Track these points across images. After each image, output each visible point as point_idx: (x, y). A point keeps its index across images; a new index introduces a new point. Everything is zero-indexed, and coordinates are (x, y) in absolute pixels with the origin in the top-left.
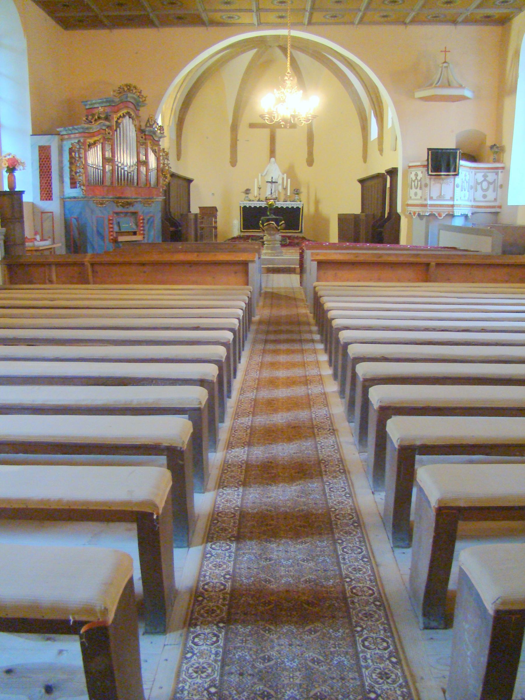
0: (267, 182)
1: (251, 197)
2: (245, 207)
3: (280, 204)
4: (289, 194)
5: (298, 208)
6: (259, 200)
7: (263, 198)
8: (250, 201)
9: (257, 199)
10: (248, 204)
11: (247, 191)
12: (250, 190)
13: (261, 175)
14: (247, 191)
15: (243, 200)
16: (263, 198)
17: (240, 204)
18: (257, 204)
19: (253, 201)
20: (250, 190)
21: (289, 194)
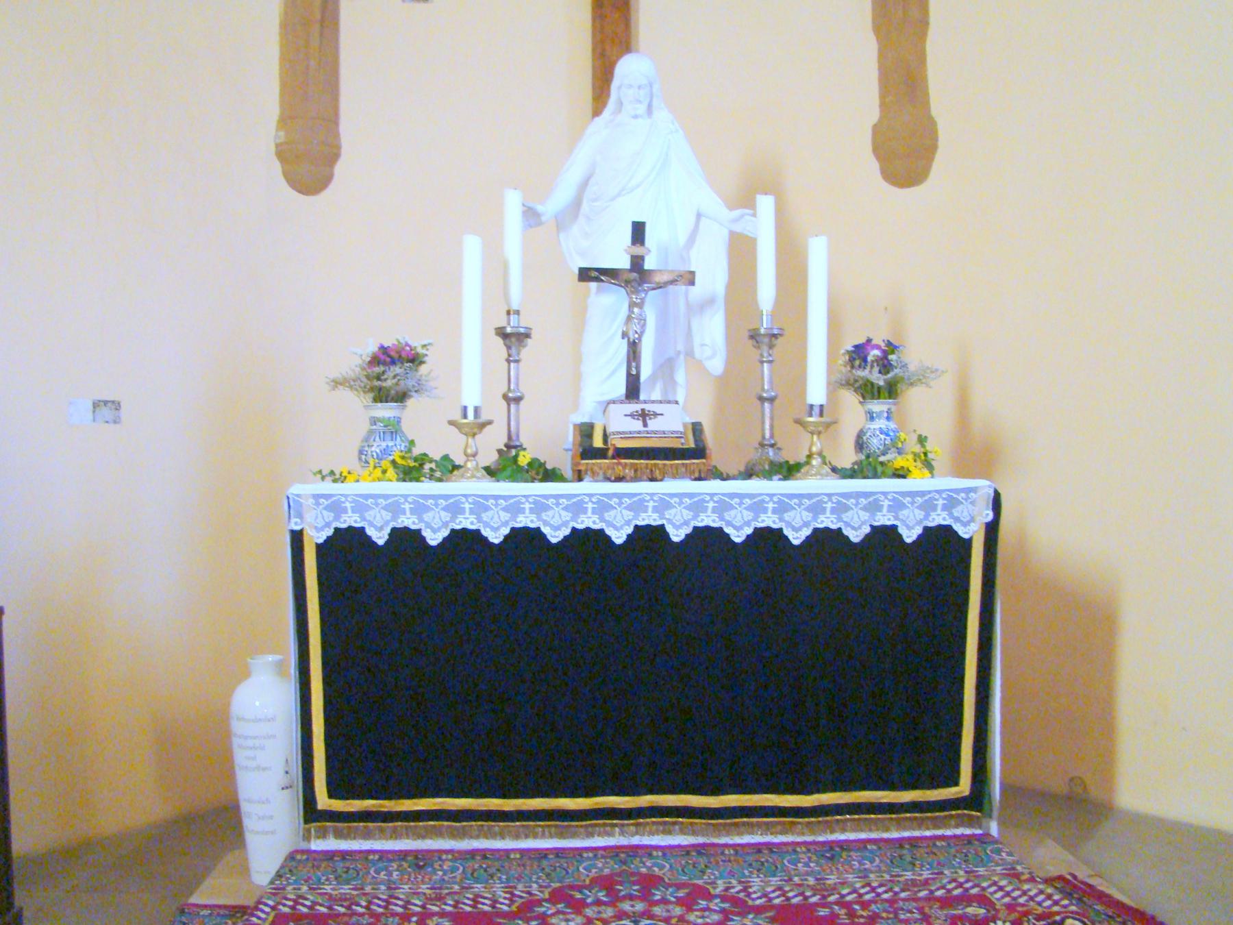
0: (586, 275)
1: (425, 426)
2: (345, 549)
3: (735, 506)
4: (817, 393)
5: (943, 545)
6: (508, 465)
7: (548, 438)
8: (411, 471)
9: (489, 445)
10: (382, 506)
11: (391, 373)
12: (415, 360)
13: (531, 216)
14: (391, 373)
15: (346, 460)
16: (548, 438)
17: (293, 506)
18: (481, 505)
19: (449, 468)
20: (415, 360)
21: (817, 393)
